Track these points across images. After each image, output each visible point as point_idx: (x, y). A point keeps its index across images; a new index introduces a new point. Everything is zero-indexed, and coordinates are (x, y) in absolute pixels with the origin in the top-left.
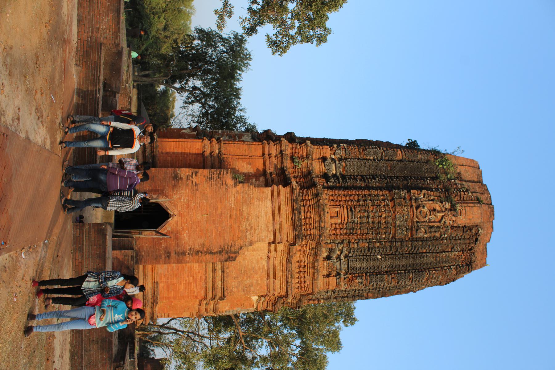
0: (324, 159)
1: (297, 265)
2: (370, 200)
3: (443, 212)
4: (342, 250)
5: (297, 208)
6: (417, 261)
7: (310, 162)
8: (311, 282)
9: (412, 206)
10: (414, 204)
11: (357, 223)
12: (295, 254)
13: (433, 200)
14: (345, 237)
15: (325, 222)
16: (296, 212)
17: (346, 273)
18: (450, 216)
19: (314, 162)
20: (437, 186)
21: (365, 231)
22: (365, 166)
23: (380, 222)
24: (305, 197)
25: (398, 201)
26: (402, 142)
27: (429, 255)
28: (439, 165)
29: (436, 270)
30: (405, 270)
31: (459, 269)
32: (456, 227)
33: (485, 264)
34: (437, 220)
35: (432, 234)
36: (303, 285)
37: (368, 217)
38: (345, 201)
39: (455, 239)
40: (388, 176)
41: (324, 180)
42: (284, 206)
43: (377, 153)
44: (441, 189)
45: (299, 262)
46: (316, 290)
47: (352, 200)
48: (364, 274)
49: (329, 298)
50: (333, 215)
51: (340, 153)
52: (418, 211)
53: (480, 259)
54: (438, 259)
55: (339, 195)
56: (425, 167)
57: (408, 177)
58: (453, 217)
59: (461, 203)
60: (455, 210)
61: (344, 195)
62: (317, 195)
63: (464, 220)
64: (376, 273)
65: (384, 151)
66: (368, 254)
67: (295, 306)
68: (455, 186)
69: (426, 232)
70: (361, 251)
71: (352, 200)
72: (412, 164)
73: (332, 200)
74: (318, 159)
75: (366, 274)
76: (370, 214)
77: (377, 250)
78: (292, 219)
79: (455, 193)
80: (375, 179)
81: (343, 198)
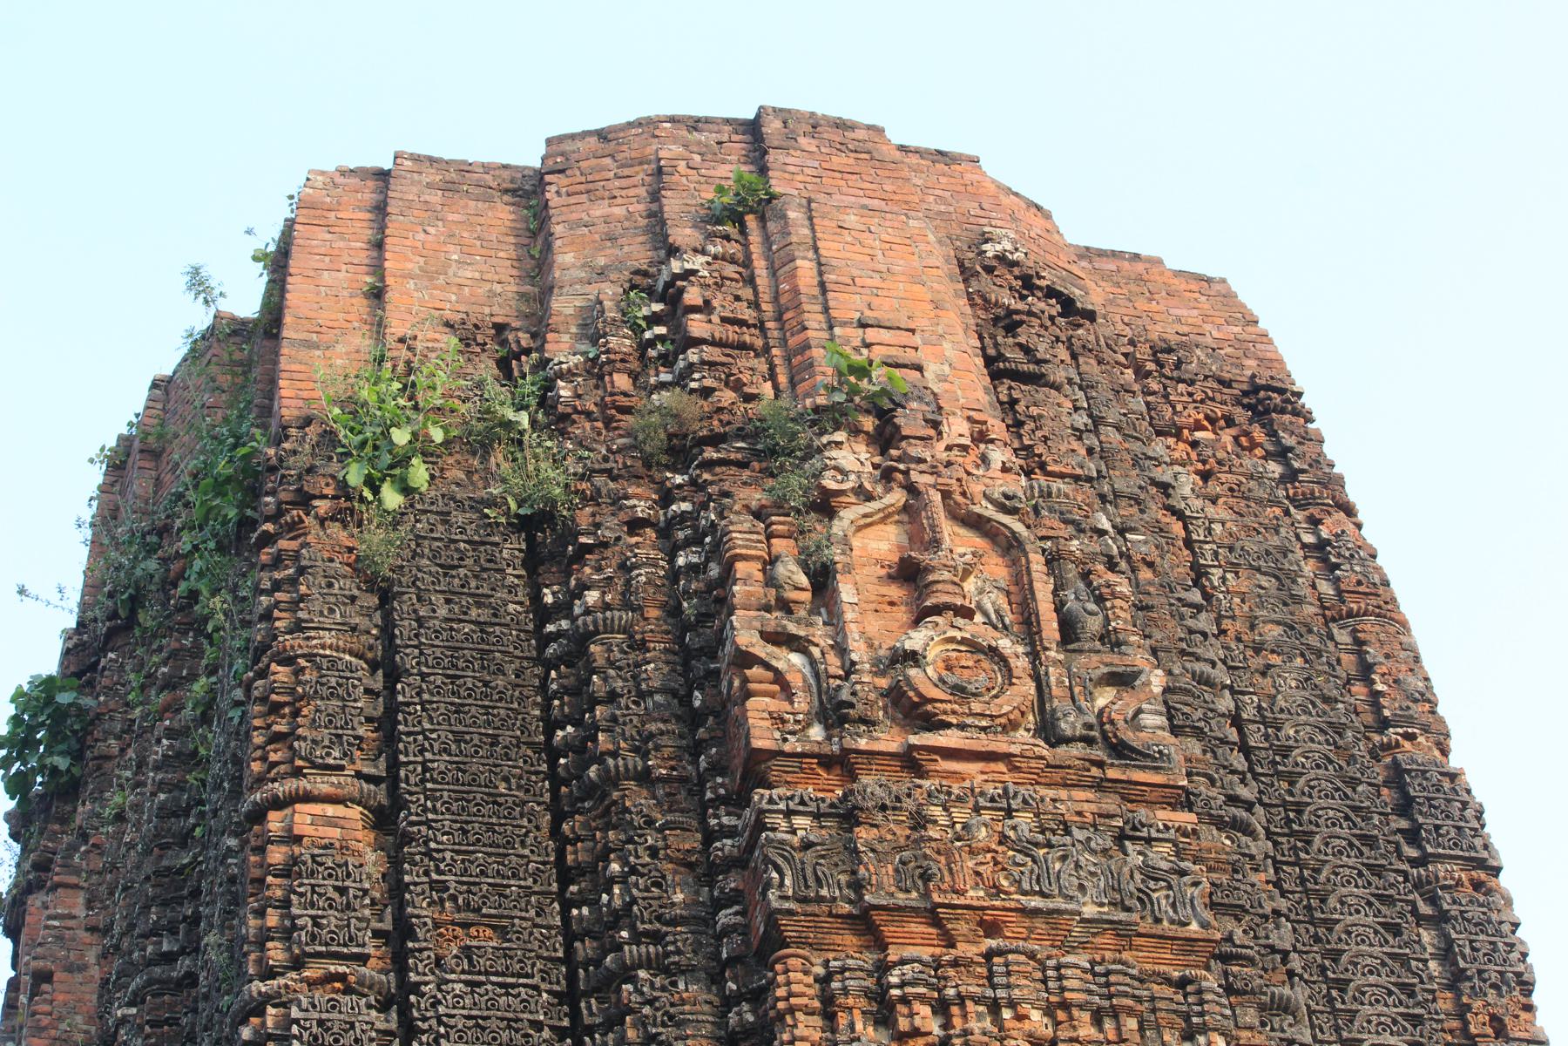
9: (911, 762)
20: (635, 525)
28: (407, 490)
52: (946, 707)
65: (297, 964)
68: (622, 381)
69: (1123, 680)
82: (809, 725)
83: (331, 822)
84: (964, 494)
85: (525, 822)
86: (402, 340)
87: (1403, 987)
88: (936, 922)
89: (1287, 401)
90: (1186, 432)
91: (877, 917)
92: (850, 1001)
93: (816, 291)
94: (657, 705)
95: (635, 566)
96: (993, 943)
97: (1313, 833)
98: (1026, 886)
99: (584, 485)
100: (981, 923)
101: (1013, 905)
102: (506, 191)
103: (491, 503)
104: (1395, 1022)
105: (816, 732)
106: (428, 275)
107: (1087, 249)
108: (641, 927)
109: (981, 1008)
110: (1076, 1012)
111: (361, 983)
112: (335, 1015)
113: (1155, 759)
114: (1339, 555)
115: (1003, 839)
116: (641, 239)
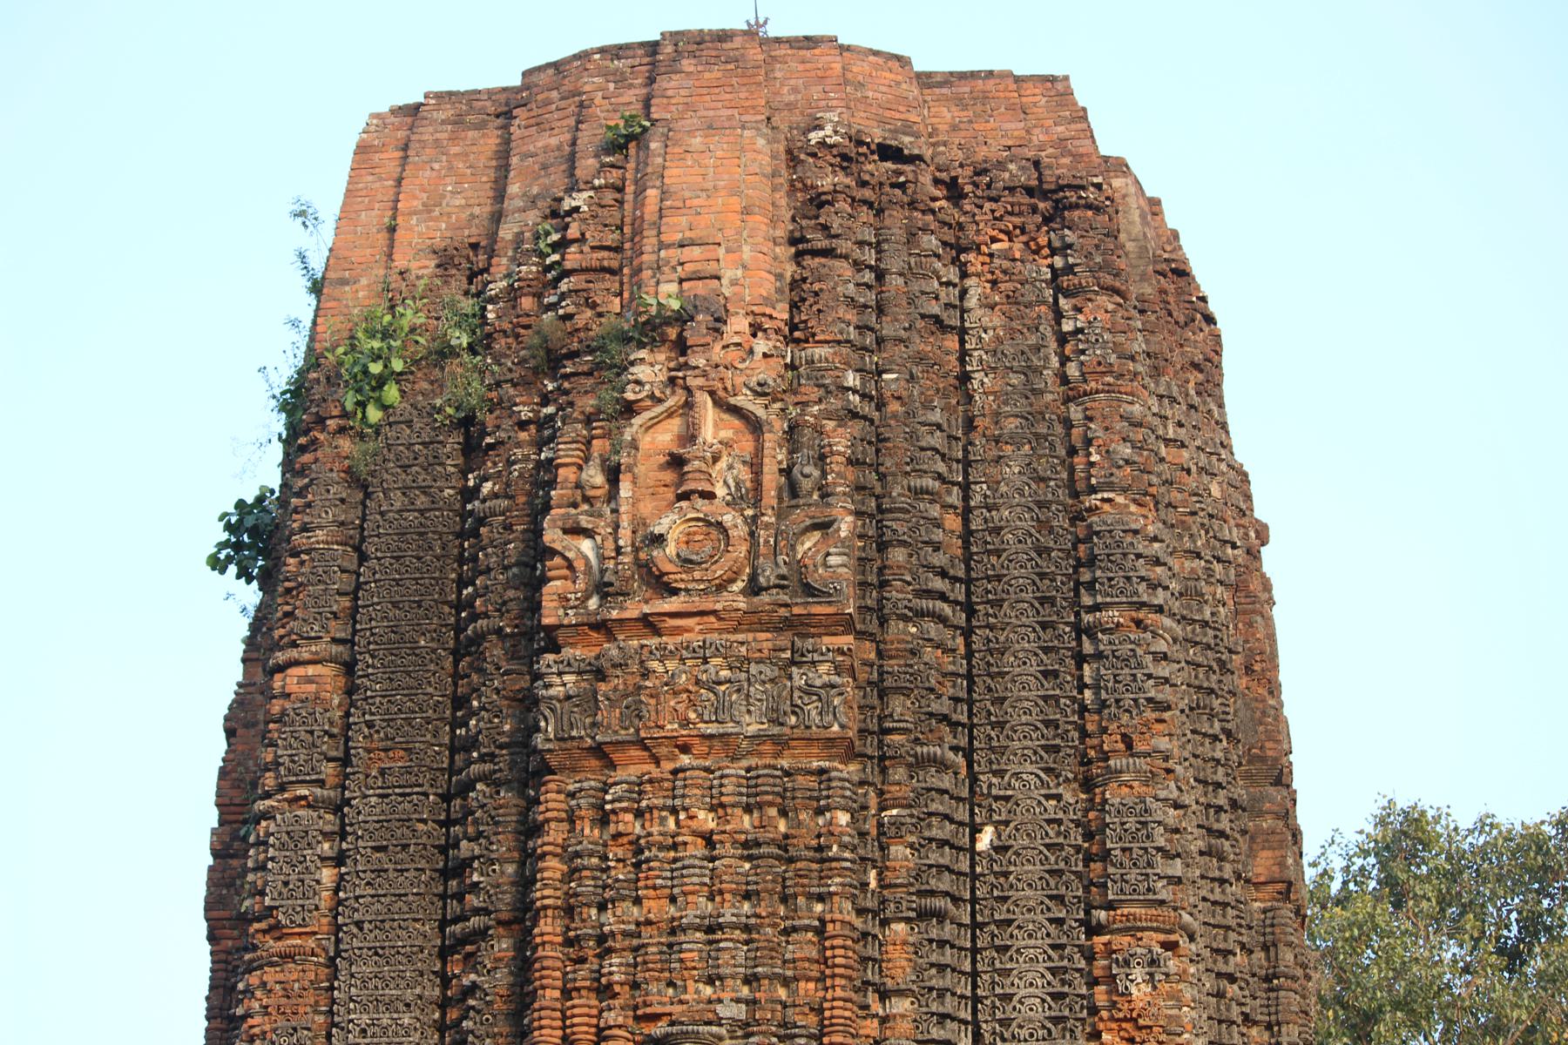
2: (602, 907)
3: (688, 405)
6: (1019, 575)
9: (649, 624)
10: (633, 609)
11: (752, 1003)
13: (613, 475)
18: (717, 353)
20: (523, 425)
21: (803, 947)
22: (379, 925)
23: (749, 847)
25: (609, 716)
27: (979, 491)
28: (384, 408)
29: (1088, 442)
30: (1080, 659)
31: (1083, 277)
32: (794, 306)
33: (1056, 88)
34: (746, 445)
35: (840, 477)
37: (712, 928)
39: (880, 310)
40: (452, 770)
43: (297, 839)
44: (545, 400)
52: (678, 578)
53: (1015, 128)
54: (1011, 424)
56: (398, 501)
57: (459, 629)
58: (730, 337)
59: (638, 271)
60: (682, 318)
63: (747, 253)
64: (1091, 866)
65: (282, 788)
66: (966, 914)
68: (527, 303)
69: (824, 526)
70: (941, 968)
72: (372, 597)
75: (1093, 930)
76: (690, 916)
77: (934, 857)
79: (568, 307)
80: (466, 864)
82: (588, 598)
83: (309, 680)
84: (725, 389)
85: (432, 667)
86: (401, 273)
87: (1048, 723)
88: (646, 748)
89: (1080, 197)
90: (984, 249)
91: (607, 749)
92: (583, 813)
93: (655, 217)
94: (514, 575)
95: (514, 463)
96: (685, 760)
97: (1003, 600)
98: (706, 718)
99: (494, 394)
100: (677, 746)
102: (498, 116)
103: (440, 411)
105: (593, 603)
106: (428, 209)
107: (951, 73)
108: (484, 750)
109: (664, 813)
110: (729, 811)
111: (316, 800)
112: (297, 827)
113: (830, 595)
114: (1087, 341)
115: (698, 682)
116: (564, 167)
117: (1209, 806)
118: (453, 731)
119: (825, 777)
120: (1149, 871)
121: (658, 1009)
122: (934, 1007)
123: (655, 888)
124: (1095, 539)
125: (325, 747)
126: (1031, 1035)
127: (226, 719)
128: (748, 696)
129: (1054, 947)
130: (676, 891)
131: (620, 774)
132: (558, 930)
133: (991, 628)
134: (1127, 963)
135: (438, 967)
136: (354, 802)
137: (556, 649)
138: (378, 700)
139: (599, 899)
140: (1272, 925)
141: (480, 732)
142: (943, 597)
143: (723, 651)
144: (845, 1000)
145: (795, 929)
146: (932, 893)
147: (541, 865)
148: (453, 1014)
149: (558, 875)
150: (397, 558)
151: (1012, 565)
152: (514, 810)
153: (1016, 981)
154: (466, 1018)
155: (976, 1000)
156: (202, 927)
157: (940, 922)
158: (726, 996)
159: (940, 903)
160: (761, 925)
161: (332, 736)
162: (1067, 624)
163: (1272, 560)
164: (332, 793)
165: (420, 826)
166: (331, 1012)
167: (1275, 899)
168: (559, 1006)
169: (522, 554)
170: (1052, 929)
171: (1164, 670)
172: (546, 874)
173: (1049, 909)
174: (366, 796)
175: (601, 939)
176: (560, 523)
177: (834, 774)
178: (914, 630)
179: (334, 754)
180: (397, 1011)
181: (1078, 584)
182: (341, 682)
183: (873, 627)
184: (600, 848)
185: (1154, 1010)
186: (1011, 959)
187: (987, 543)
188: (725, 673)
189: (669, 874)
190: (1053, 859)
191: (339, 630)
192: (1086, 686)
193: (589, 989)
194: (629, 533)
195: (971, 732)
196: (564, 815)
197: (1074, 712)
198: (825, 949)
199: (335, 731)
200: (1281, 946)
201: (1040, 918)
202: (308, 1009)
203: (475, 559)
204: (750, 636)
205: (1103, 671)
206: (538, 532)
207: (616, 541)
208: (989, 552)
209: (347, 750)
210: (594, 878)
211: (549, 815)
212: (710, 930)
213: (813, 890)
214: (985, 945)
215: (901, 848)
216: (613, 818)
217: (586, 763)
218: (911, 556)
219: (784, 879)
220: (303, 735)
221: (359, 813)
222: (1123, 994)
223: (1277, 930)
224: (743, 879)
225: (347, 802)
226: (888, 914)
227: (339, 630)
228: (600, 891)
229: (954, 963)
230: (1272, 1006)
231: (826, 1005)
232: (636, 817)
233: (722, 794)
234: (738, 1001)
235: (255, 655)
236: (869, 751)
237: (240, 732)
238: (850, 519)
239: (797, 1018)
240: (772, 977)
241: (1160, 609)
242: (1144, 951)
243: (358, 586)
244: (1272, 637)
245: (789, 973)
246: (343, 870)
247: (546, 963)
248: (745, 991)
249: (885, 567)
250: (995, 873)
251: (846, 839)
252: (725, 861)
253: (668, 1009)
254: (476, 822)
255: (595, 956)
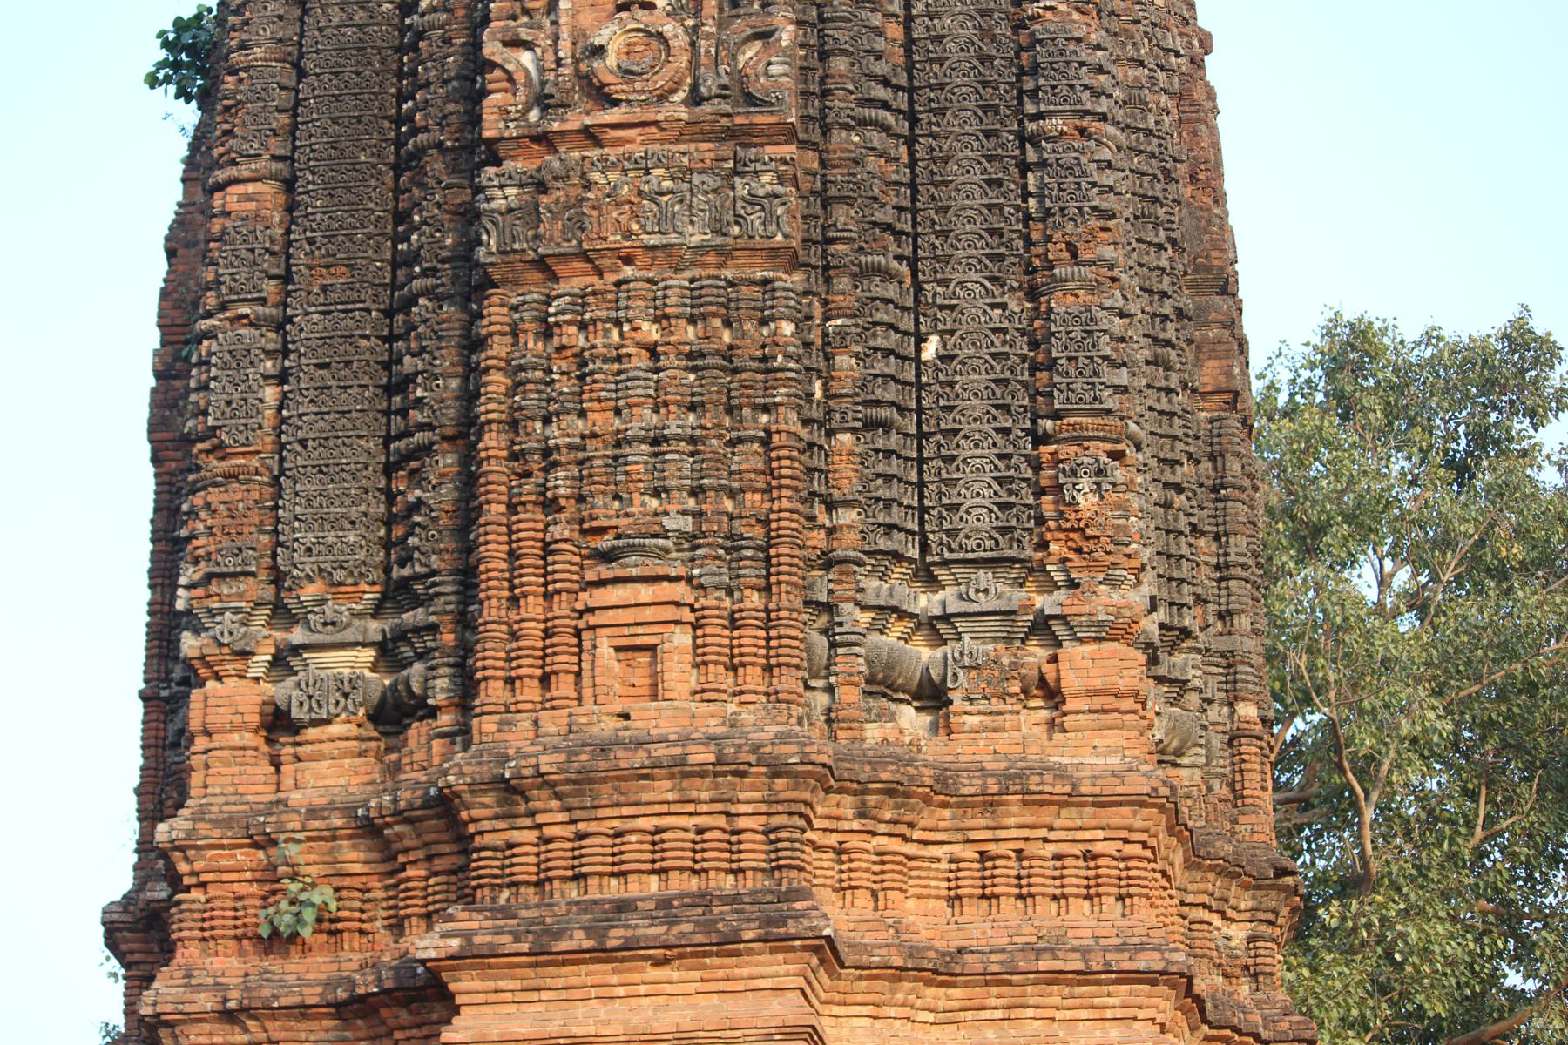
0: (278, 723)
1: (973, 911)
2: (547, 421)
4: (881, 608)
5: (589, 931)
6: (962, 83)
7: (294, 822)
8: (1088, 815)
9: (590, 135)
11: (698, 515)
12: (896, 927)
14: (787, 598)
15: (685, 740)
16: (615, 938)
17: (1037, 571)
19: (295, 797)
21: (749, 458)
22: (323, 442)
24: (526, 865)
26: (172, 127)
30: (1024, 168)
36: (1109, 871)
38: (547, 596)
40: (394, 286)
41: (416, 732)
42: (580, 1010)
43: (240, 358)
45: (954, 900)
46: (1138, 784)
47: (547, 549)
48: (1046, 450)
49: (1229, 659)
50: (641, 678)
51: (237, 613)
52: (618, 89)
55: (514, 636)
57: (399, 143)
61: (514, 601)
62: (510, 790)
64: (1037, 376)
65: (223, 307)
66: (913, 424)
67: (1273, 899)
69: (765, 35)
70: (888, 478)
71: (547, 549)
72: (314, 116)
73: (545, 680)
74: (276, 764)
75: (1040, 439)
76: (635, 428)
77: (879, 367)
78: (658, 963)
80: (410, 379)
81: (533, 607)
82: (528, 110)
83: (249, 198)
85: (373, 182)
87: (992, 232)
88: (589, 260)
91: (549, 262)
92: (526, 326)
96: (629, 271)
97: (946, 109)
98: (649, 229)
100: (620, 258)
101: (637, 244)
104: (980, 262)
105: (534, 115)
108: (426, 265)
110: (673, 322)
111: (258, 319)
112: (240, 346)
113: (772, 105)
115: (640, 193)
117: (1154, 315)
118: (394, 246)
119: (769, 287)
120: (1095, 380)
121: (604, 523)
122: (881, 518)
123: (599, 400)
124: (1038, 47)
125: (266, 265)
126: (979, 545)
127: (167, 239)
128: (691, 206)
129: (1000, 456)
130: (621, 403)
131: (563, 287)
132: (503, 444)
133: (935, 136)
134: (1074, 473)
135: (383, 484)
136: (296, 320)
137: (497, 162)
138: (318, 216)
139: (543, 412)
140: (1219, 435)
141: (422, 247)
142: (885, 106)
143: (665, 162)
144: (792, 511)
145: (740, 441)
146: (878, 403)
147: (484, 379)
148: (398, 531)
149: (502, 389)
150: (336, 74)
151: (954, 74)
152: (457, 325)
153: (963, 491)
154: (412, 534)
155: (923, 510)
156: (146, 449)
157: (886, 432)
158: (672, 508)
159: (885, 413)
160: (707, 437)
161: (273, 253)
162: (1010, 132)
163: (1214, 68)
164: (274, 311)
165: (363, 343)
166: (276, 532)
167: (1221, 409)
168: (504, 520)
169: (461, 67)
170: (998, 438)
171: (1108, 178)
172: (490, 389)
173: (995, 419)
174: (308, 313)
175: (546, 452)
176: (499, 36)
177: (778, 284)
178: (857, 139)
179: (275, 271)
180: (342, 529)
181: (1021, 92)
182: (282, 199)
183: (816, 136)
184: (543, 361)
185: (1101, 520)
186: (958, 469)
187: (929, 51)
188: (667, 184)
189: (613, 386)
190: (998, 368)
191: (279, 147)
192: (1031, 194)
193: (534, 503)
194: (569, 44)
195: (915, 241)
196: (507, 329)
197: (1018, 221)
198: (771, 460)
199: (276, 248)
200: (1228, 455)
201: (986, 427)
202: (253, 529)
203: (414, 73)
204: (692, 147)
205: (1047, 180)
206: (477, 45)
207: (556, 53)
208: (932, 61)
209: (288, 266)
210: (538, 392)
211: (492, 328)
212: (655, 442)
213: (758, 401)
214: (931, 455)
215: (845, 358)
216: (556, 330)
217: (529, 276)
218: (853, 65)
219: (729, 390)
220: (244, 254)
221: (301, 330)
222: (1070, 504)
223: (1224, 440)
224: (688, 391)
225: (289, 320)
226: (834, 424)
227: (279, 147)
228: (544, 404)
229: (901, 473)
230: (1219, 517)
231: (773, 516)
232: (580, 329)
233: (665, 305)
234: (684, 513)
235: (194, 174)
236: (813, 261)
237: (180, 252)
238: (791, 28)
239: (743, 530)
240: (718, 489)
241: (1103, 117)
242: (1092, 461)
243: (298, 103)
244: (1216, 146)
245: (736, 485)
246: (286, 388)
247: (491, 478)
248: (691, 503)
249: (827, 76)
250: (941, 383)
251: (791, 349)
252: (670, 373)
253: (614, 522)
254: (419, 337)
255: (541, 469)
